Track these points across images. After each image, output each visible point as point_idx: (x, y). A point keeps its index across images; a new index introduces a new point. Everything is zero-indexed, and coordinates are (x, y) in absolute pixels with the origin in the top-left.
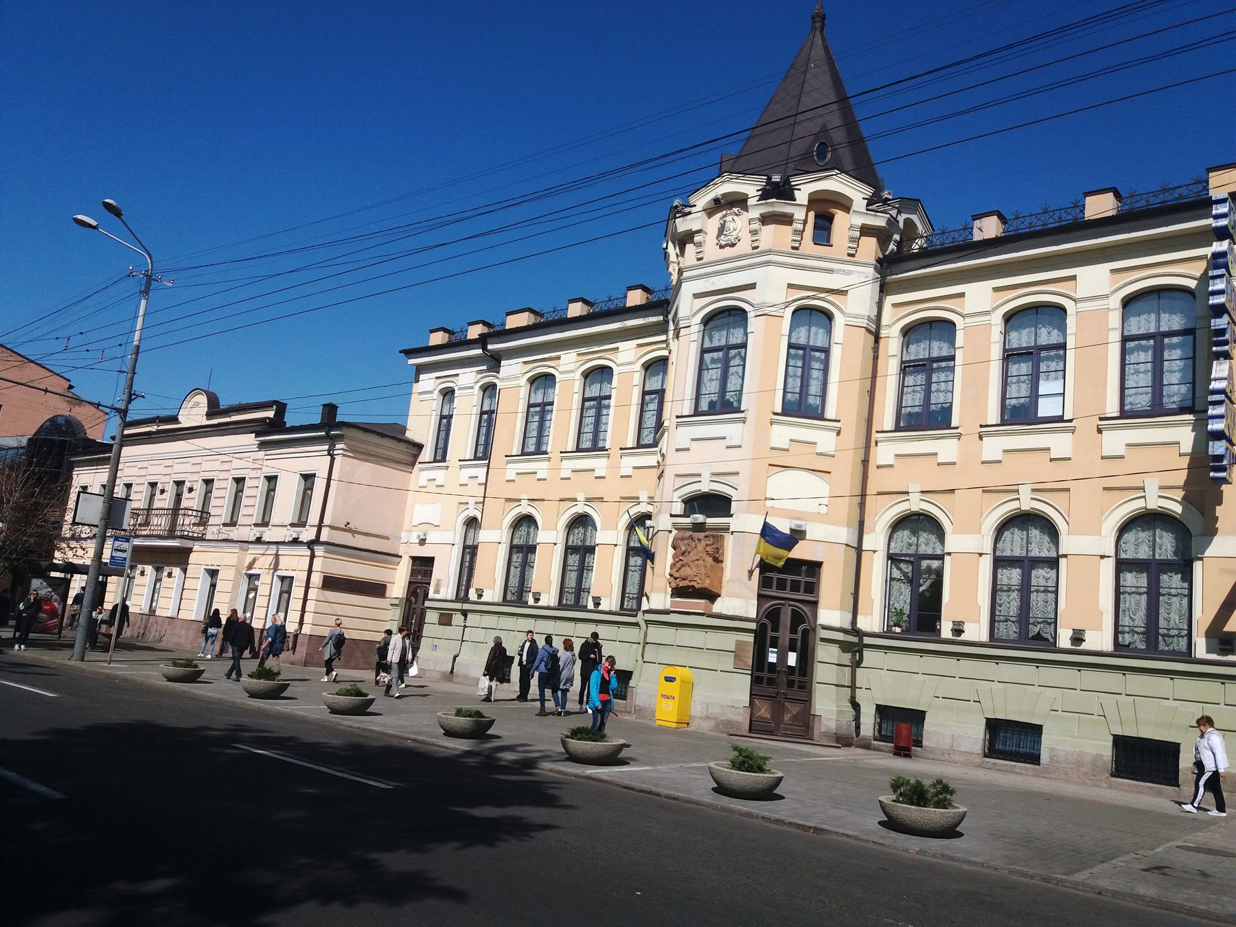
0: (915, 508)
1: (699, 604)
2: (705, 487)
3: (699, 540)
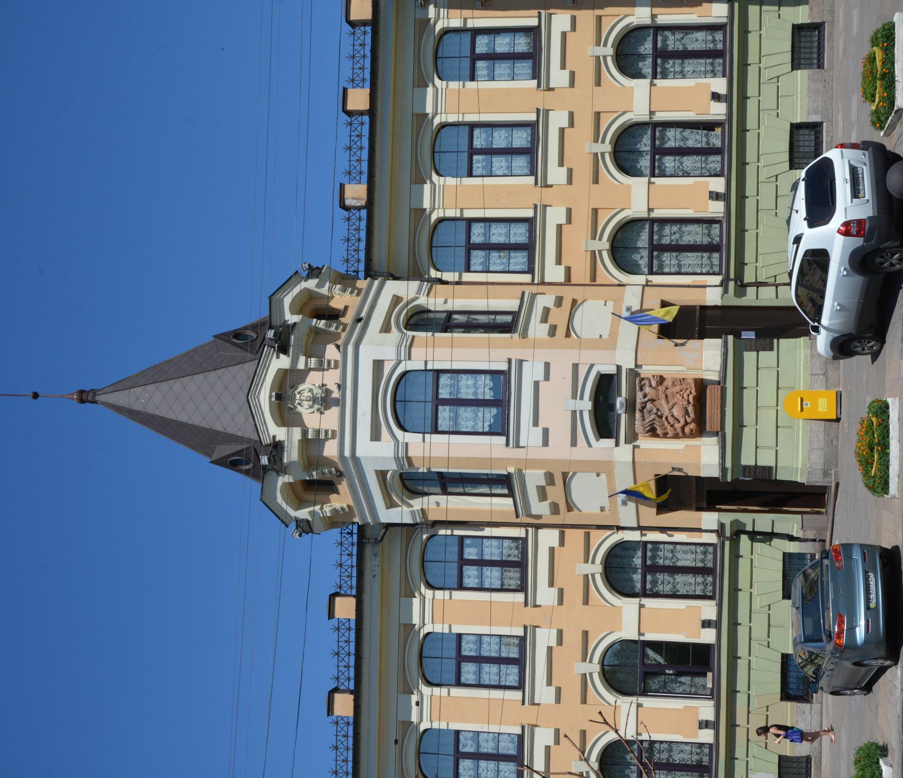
0: (607, 246)
1: (712, 395)
2: (586, 405)
3: (645, 396)
